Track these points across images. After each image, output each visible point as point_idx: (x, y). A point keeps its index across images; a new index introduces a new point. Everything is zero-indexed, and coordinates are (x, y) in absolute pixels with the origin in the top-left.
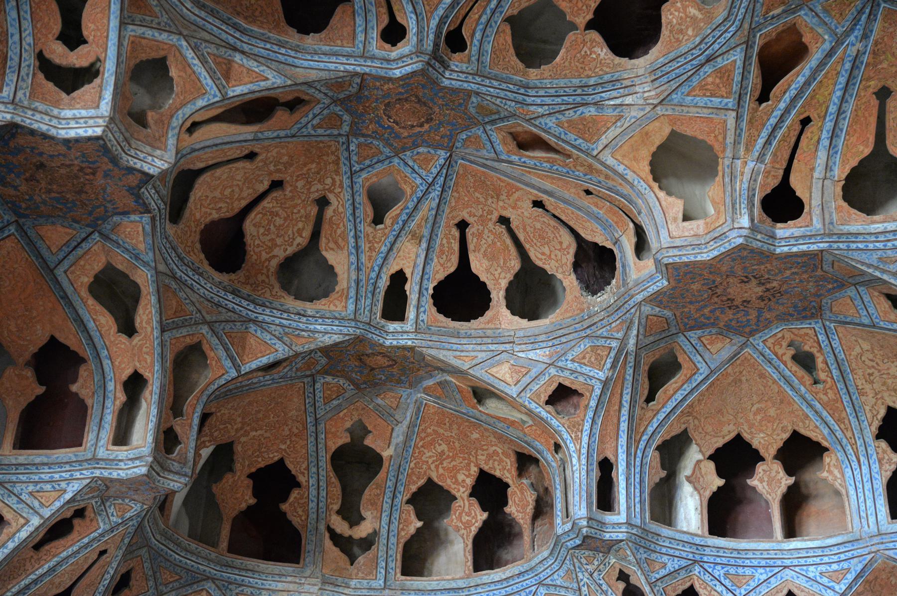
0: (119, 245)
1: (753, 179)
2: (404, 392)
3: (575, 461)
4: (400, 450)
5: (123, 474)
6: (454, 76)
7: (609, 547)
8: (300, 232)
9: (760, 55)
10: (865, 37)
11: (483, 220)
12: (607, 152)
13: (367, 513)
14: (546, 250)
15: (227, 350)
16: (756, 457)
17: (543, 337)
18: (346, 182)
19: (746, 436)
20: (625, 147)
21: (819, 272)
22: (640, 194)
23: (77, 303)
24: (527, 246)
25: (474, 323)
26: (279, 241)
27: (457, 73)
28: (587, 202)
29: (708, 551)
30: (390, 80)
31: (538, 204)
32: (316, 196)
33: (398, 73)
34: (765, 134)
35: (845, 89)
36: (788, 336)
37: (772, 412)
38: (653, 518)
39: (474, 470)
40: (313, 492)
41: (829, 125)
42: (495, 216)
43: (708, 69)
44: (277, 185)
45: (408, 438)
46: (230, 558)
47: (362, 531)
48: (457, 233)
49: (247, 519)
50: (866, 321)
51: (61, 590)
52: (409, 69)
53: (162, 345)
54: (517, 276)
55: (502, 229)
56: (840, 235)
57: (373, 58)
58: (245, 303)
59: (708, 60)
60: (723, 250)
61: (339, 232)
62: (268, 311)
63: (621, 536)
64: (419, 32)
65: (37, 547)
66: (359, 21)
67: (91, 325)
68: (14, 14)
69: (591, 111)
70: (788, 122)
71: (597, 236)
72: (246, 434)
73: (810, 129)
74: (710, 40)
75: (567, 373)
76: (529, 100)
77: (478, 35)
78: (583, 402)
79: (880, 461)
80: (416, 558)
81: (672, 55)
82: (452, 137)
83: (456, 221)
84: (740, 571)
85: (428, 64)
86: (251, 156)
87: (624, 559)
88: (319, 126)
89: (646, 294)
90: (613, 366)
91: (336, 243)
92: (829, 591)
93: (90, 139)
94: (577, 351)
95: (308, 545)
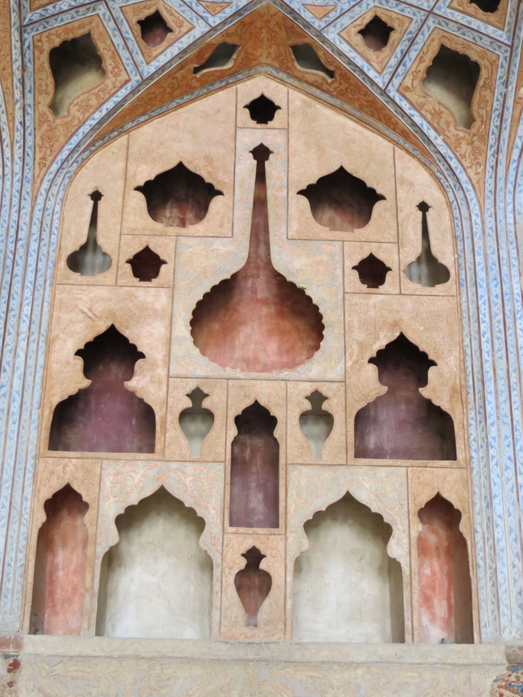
92: (201, 21)
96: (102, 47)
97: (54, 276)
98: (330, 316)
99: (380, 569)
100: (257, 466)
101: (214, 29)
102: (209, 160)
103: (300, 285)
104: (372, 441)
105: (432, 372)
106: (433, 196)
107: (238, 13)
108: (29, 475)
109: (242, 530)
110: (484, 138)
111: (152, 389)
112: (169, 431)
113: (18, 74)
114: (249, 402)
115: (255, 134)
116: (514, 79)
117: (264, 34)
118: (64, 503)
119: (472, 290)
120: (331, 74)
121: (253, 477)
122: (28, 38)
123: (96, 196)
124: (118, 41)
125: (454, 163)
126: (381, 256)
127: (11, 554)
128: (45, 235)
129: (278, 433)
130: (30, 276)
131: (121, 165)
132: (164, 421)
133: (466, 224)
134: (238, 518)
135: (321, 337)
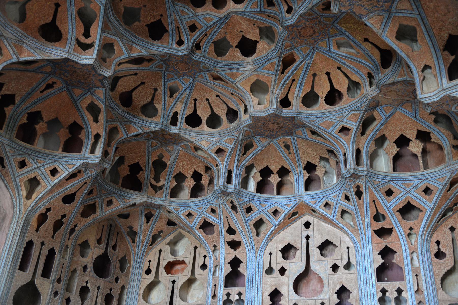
0: (95, 97)
1: (278, 95)
2: (175, 146)
3: (221, 170)
5: (92, 162)
6: (197, 57)
7: (229, 194)
8: (148, 97)
9: (283, 60)
10: (311, 59)
11: (202, 99)
12: (239, 83)
13: (161, 180)
15: (124, 129)
16: (271, 172)
17: (216, 134)
18: (163, 84)
19: (269, 166)
20: (244, 82)
21: (293, 123)
22: (246, 96)
23: (82, 112)
24: (213, 108)
25: (196, 128)
26: (142, 100)
27: (197, 56)
28: (231, 97)
29: (256, 197)
30: (178, 56)
31: (218, 96)
32: (154, 87)
33: (180, 54)
34: (282, 83)
35: (305, 73)
36: (284, 140)
38: (242, 187)
39: (193, 170)
41: (300, 82)
42: (205, 98)
43: (268, 62)
44: (143, 83)
45: (175, 159)
47: (160, 184)
49: (126, 178)
50: (304, 137)
51: (73, 192)
52: (184, 53)
53: (106, 126)
54: (210, 116)
55: (207, 102)
56: (300, 113)
57: (174, 49)
58: (131, 117)
59: (269, 60)
62: (137, 119)
63: (232, 191)
64: (188, 43)
65: (67, 180)
66: (171, 38)
67: (86, 119)
68: (71, 27)
69: (235, 71)
70: (289, 80)
72: (128, 154)
74: (270, 54)
75: (221, 145)
76: (218, 66)
77: (204, 46)
78: (225, 153)
80: (174, 193)
81: (259, 58)
82: (195, 74)
84: (264, 203)
85: (189, 52)
86: (136, 74)
87: (233, 197)
88: (156, 67)
90: (235, 144)
91: (159, 102)
93: (89, 64)
94: (225, 139)
95: (144, 187)
97: (262, 276)
98: (325, 281)
101: (290, 210)
105: (351, 295)
113: (247, 231)
115: (306, 232)
116: (360, 217)
122: (247, 223)
124: (268, 218)
128: (260, 266)
130: (257, 277)
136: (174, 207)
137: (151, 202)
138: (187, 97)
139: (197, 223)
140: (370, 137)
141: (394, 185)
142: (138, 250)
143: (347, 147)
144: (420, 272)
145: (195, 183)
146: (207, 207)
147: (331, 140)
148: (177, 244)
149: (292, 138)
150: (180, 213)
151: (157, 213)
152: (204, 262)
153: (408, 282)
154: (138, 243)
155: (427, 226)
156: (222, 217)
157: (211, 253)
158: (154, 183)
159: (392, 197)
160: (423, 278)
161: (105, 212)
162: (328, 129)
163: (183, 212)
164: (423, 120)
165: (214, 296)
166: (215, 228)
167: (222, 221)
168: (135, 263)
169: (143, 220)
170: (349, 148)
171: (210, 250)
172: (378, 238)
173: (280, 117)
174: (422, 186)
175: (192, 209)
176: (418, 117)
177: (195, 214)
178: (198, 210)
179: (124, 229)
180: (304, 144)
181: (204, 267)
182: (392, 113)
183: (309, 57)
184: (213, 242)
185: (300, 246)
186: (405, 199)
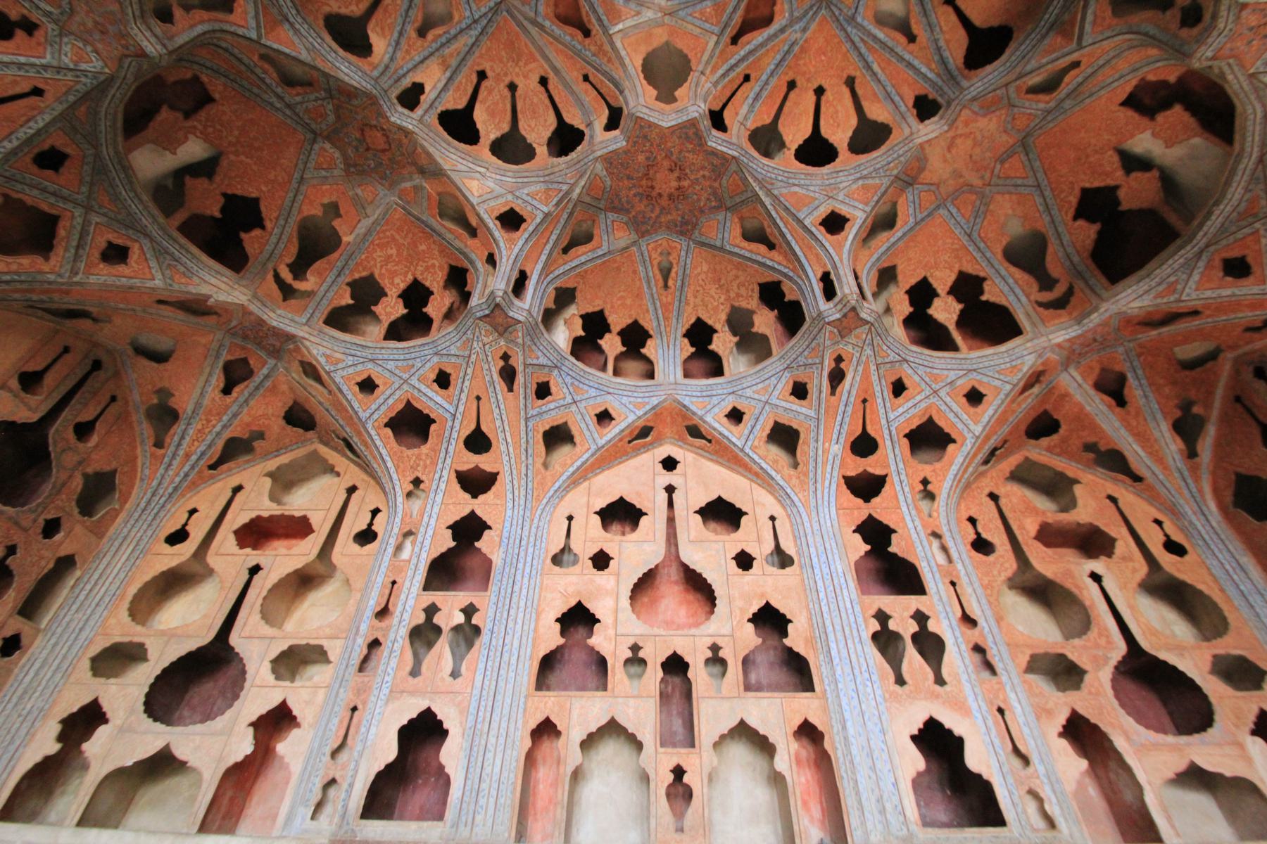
2: (382, 191)
3: (504, 260)
4: (358, 240)
10: (804, 30)
12: (620, 35)
14: (533, 123)
21: (716, 185)
24: (520, 116)
31: (543, 81)
34: (726, 67)
35: (777, 65)
37: (629, 302)
39: (410, 278)
40: (274, 239)
41: (757, 89)
42: (507, 80)
46: (176, 234)
48: (474, 78)
50: (718, 244)
60: (680, 121)
61: (389, 21)
62: (306, 26)
63: (521, 318)
71: (574, 118)
72: (237, 154)
73: (746, 85)
78: (524, 226)
79: (681, 349)
80: (339, 319)
83: (479, 68)
89: (605, 151)
90: (557, 205)
95: (252, 266)
96: (575, 432)
99: (769, 778)
100: (677, 699)
101: (639, 418)
102: (638, 494)
103: (698, 571)
104: (753, 678)
106: (778, 511)
107: (653, 408)
108: (521, 710)
109: (670, 750)
110: (806, 474)
111: (605, 644)
112: (617, 672)
114: (670, 652)
115: (667, 478)
117: (669, 419)
118: (546, 730)
119: (810, 571)
120: (710, 441)
121: (674, 707)
123: (570, 518)
124: (583, 426)
125: (789, 491)
126: (748, 550)
127: (505, 774)
128: (538, 543)
129: (690, 674)
130: (528, 570)
131: (585, 499)
132: (614, 667)
133: (801, 528)
134: (666, 741)
135: (714, 605)
136: (328, 352)
137: (260, 313)
138: (462, 55)
139: (383, 408)
140: (875, 256)
141: (910, 371)
142: (167, 470)
143: (836, 259)
144: (958, 577)
145: (405, 311)
146: (428, 365)
147: (793, 243)
148: (294, 490)
149: (684, 244)
150: (340, 373)
151: (265, 371)
152: (371, 524)
153: (936, 598)
154: (172, 449)
155: (958, 479)
156: (464, 396)
157: (400, 499)
158: (286, 275)
159: (901, 399)
160: (969, 590)
161: (88, 273)
162: (799, 211)
163: (351, 370)
164: (982, 245)
165: (383, 613)
166: (433, 427)
167: (461, 408)
168: (143, 504)
169: (214, 381)
170: (841, 260)
171: (398, 488)
172: (852, 496)
173: (700, 140)
174: (964, 384)
175: (380, 369)
176: (975, 235)
177: (385, 384)
178: (397, 372)
179: (141, 394)
180: (705, 268)
181: (366, 537)
182: (928, 216)
183: (802, 24)
184: (414, 468)
185: (650, 505)
186: (927, 409)
